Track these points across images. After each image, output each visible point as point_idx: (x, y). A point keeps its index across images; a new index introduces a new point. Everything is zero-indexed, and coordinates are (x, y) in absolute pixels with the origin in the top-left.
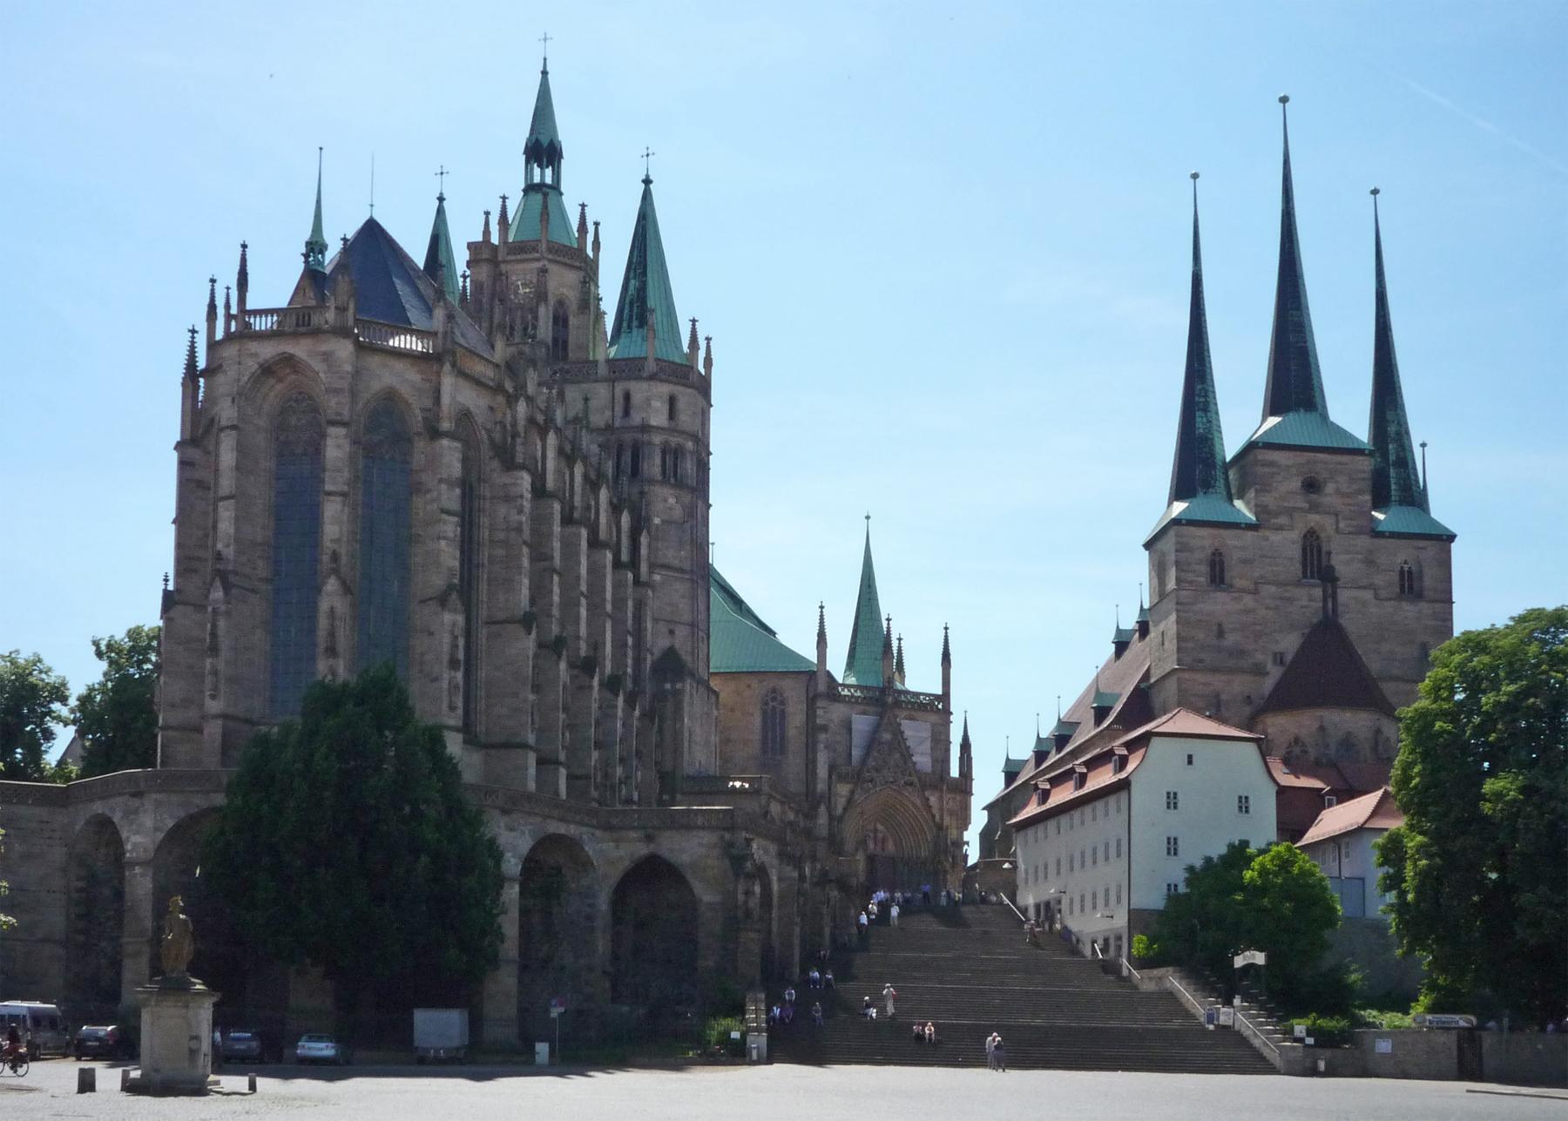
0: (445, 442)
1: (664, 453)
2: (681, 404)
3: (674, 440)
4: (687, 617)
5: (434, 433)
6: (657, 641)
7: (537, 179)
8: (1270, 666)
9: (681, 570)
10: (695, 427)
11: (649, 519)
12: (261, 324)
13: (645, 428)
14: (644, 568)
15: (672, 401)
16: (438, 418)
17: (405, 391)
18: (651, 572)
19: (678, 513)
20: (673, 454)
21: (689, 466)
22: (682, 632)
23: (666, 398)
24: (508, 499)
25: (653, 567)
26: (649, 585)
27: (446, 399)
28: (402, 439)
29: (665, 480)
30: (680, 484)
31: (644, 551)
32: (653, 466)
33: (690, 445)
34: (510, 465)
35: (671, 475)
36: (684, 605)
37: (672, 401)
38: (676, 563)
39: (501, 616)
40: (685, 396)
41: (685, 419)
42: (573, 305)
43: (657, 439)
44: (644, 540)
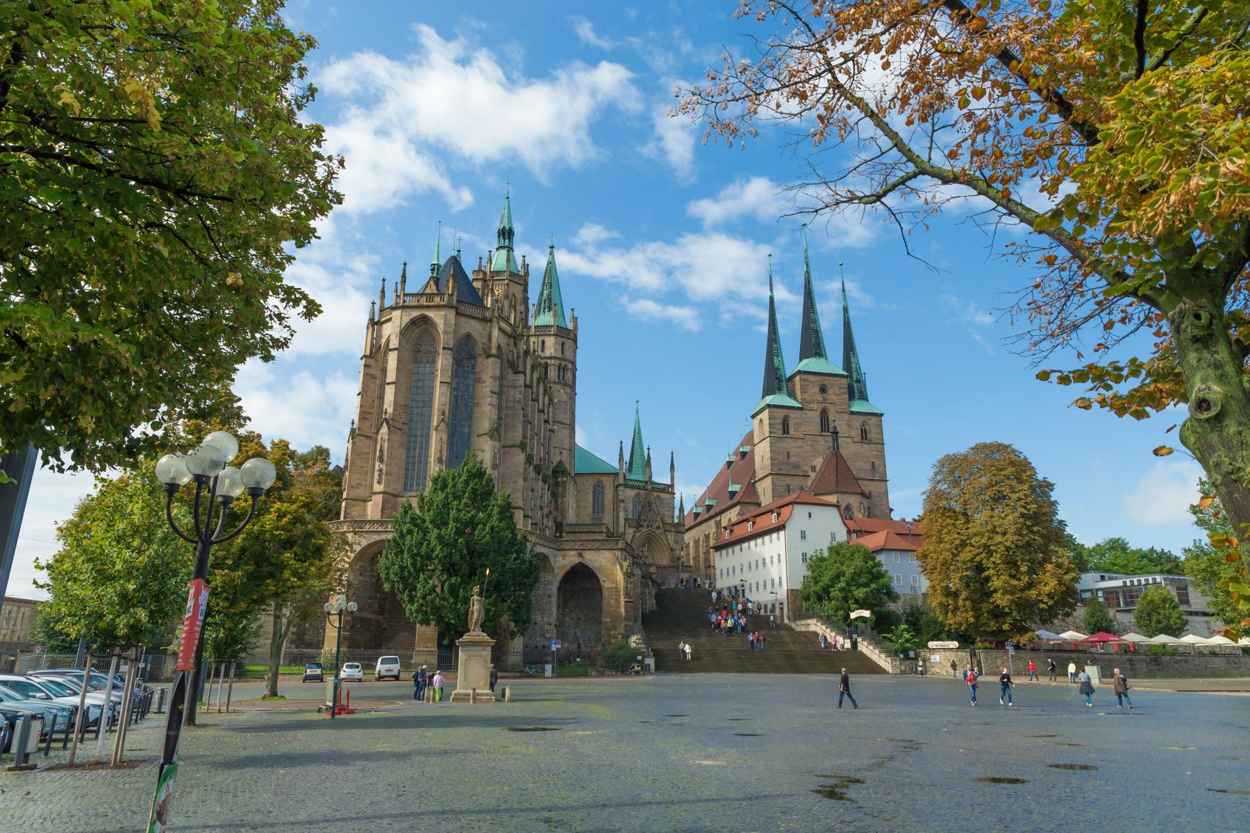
0: (492, 359)
2: (566, 347)
4: (567, 446)
5: (489, 356)
6: (556, 459)
8: (810, 473)
10: (571, 359)
12: (410, 301)
13: (551, 358)
16: (490, 348)
20: (562, 369)
21: (569, 375)
22: (565, 453)
24: (515, 387)
27: (494, 339)
28: (472, 357)
29: (559, 383)
30: (566, 385)
32: (552, 374)
33: (570, 366)
36: (567, 441)
39: (510, 443)
40: (568, 343)
41: (568, 355)
43: (557, 362)
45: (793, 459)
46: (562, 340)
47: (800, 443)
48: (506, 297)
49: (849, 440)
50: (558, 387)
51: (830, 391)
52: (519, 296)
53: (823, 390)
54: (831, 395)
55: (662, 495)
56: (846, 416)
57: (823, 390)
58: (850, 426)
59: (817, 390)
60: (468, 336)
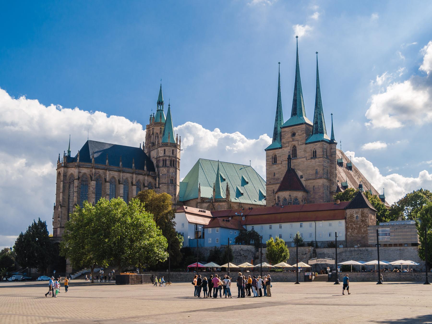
1: (164, 161)
2: (166, 151)
3: (164, 158)
7: (159, 109)
9: (165, 183)
11: (159, 175)
13: (160, 157)
14: (157, 185)
15: (165, 150)
17: (73, 173)
18: (159, 185)
19: (166, 172)
23: (163, 150)
25: (159, 184)
26: (159, 188)
29: (163, 166)
31: (157, 181)
32: (161, 164)
34: (92, 180)
35: (165, 165)
37: (165, 150)
38: (165, 182)
40: (167, 148)
42: (159, 133)
43: (161, 159)
44: (157, 179)
45: (277, 176)
46: (163, 148)
47: (280, 166)
48: (153, 134)
49: (305, 159)
50: (161, 169)
51: (297, 134)
52: (158, 132)
53: (294, 134)
54: (297, 137)
55: (221, 204)
56: (304, 146)
57: (294, 134)
58: (305, 151)
59: (290, 135)
60: (72, 174)
